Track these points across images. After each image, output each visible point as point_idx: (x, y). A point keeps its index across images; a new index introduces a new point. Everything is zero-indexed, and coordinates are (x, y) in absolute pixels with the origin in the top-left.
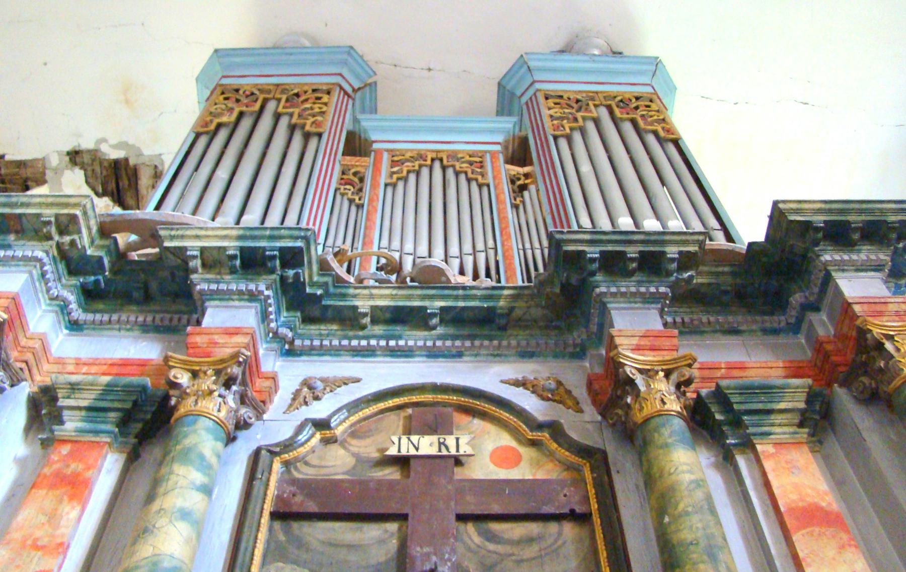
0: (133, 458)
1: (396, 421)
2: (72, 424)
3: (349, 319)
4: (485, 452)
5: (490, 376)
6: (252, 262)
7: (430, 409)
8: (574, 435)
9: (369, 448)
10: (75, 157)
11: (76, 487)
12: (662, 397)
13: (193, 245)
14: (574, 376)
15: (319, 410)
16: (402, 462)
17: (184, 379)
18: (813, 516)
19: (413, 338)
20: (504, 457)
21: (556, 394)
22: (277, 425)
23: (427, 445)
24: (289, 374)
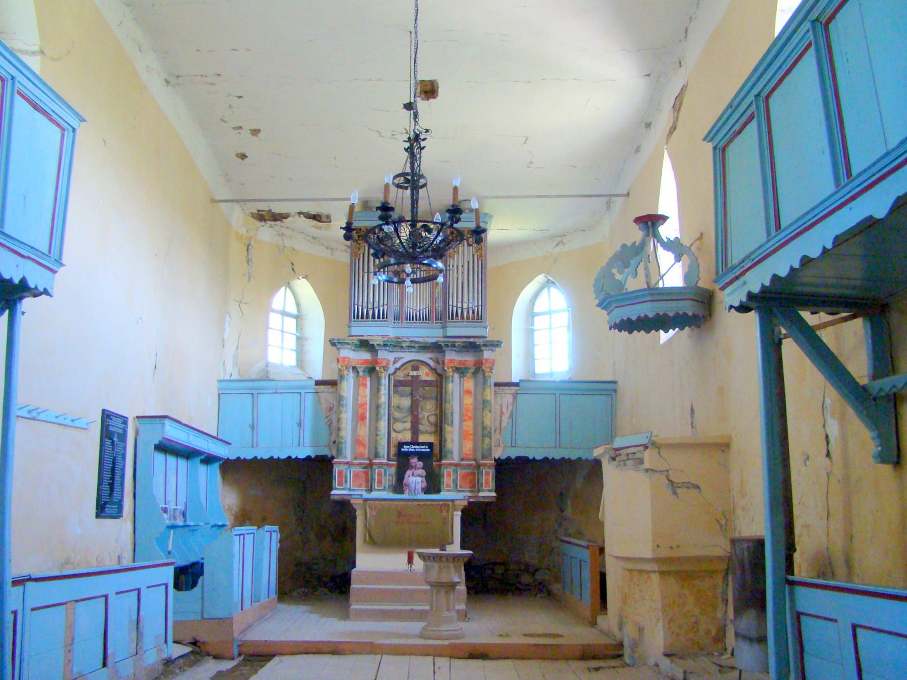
0: (371, 377)
1: (410, 368)
2: (361, 374)
3: (402, 347)
4: (424, 374)
5: (425, 357)
6: (385, 345)
7: (416, 365)
8: (438, 371)
9: (406, 372)
10: (300, 213)
11: (365, 385)
12: (450, 372)
13: (375, 343)
14: (439, 356)
15: (398, 365)
16: (412, 377)
17: (378, 368)
18: (468, 392)
19: (412, 350)
20: (427, 375)
21: (437, 362)
22: (391, 371)
23: (415, 373)
24: (391, 357)
